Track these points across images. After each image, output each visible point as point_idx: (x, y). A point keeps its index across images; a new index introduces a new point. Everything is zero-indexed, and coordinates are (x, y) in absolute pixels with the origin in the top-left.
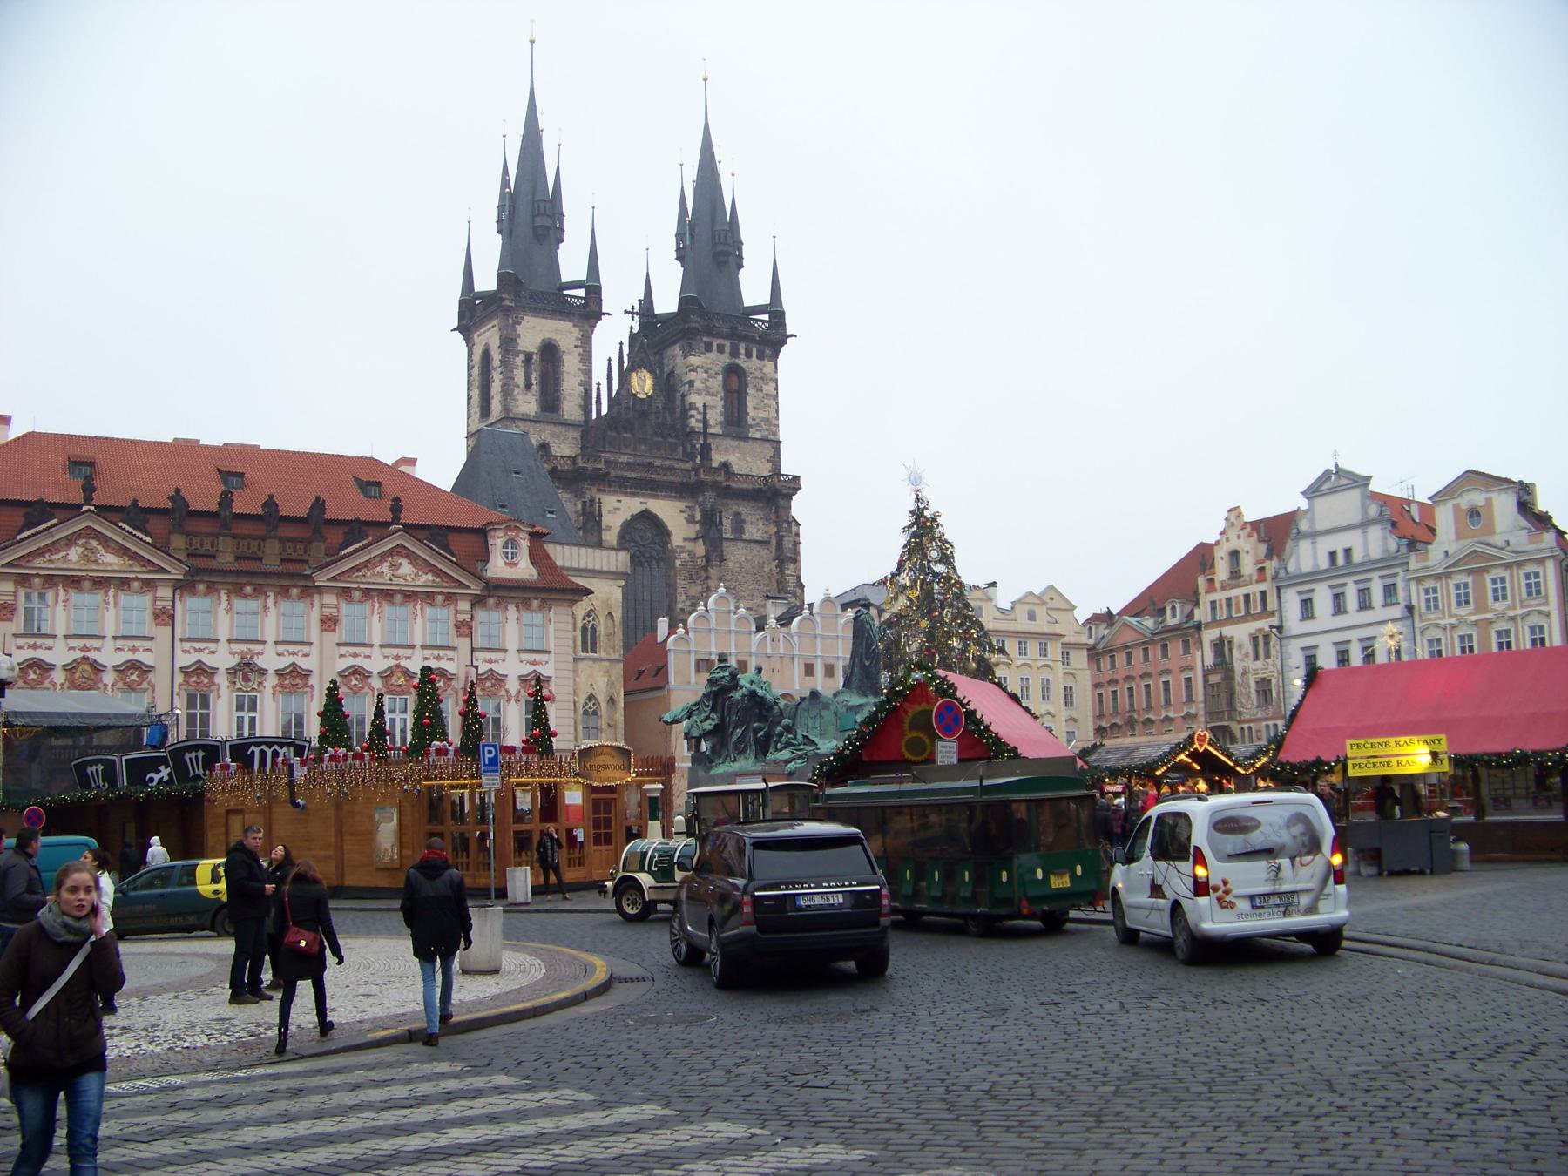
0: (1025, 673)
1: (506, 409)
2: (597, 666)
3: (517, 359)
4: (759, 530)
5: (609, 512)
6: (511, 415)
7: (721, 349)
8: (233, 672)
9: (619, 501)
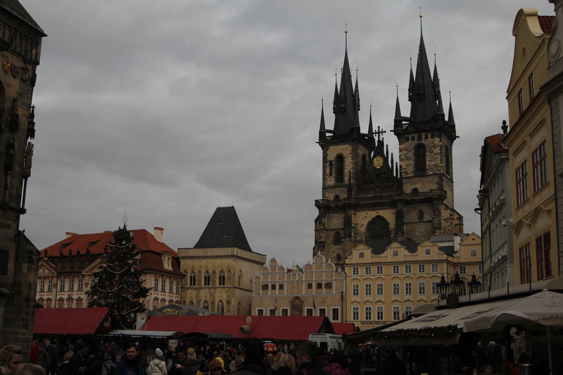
0: (422, 281)
1: (324, 185)
2: (223, 290)
4: (431, 216)
5: (363, 219)
6: (325, 187)
7: (413, 139)
8: (67, 300)
9: (367, 213)
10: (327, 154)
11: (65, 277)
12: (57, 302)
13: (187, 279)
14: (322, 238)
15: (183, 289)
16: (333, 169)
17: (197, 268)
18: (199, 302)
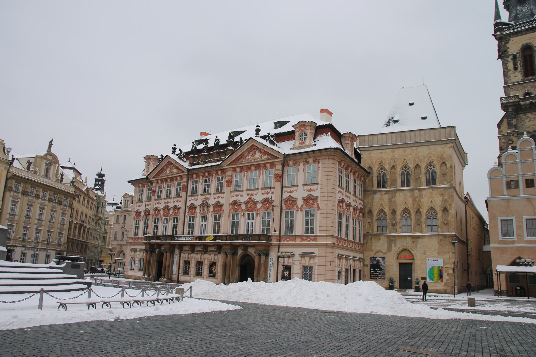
2: (435, 192)
3: (508, 59)
8: (200, 206)
10: (508, 47)
11: (198, 176)
12: (187, 210)
13: (373, 179)
14: (513, 143)
15: (368, 193)
16: (517, 62)
17: (387, 162)
18: (394, 212)
